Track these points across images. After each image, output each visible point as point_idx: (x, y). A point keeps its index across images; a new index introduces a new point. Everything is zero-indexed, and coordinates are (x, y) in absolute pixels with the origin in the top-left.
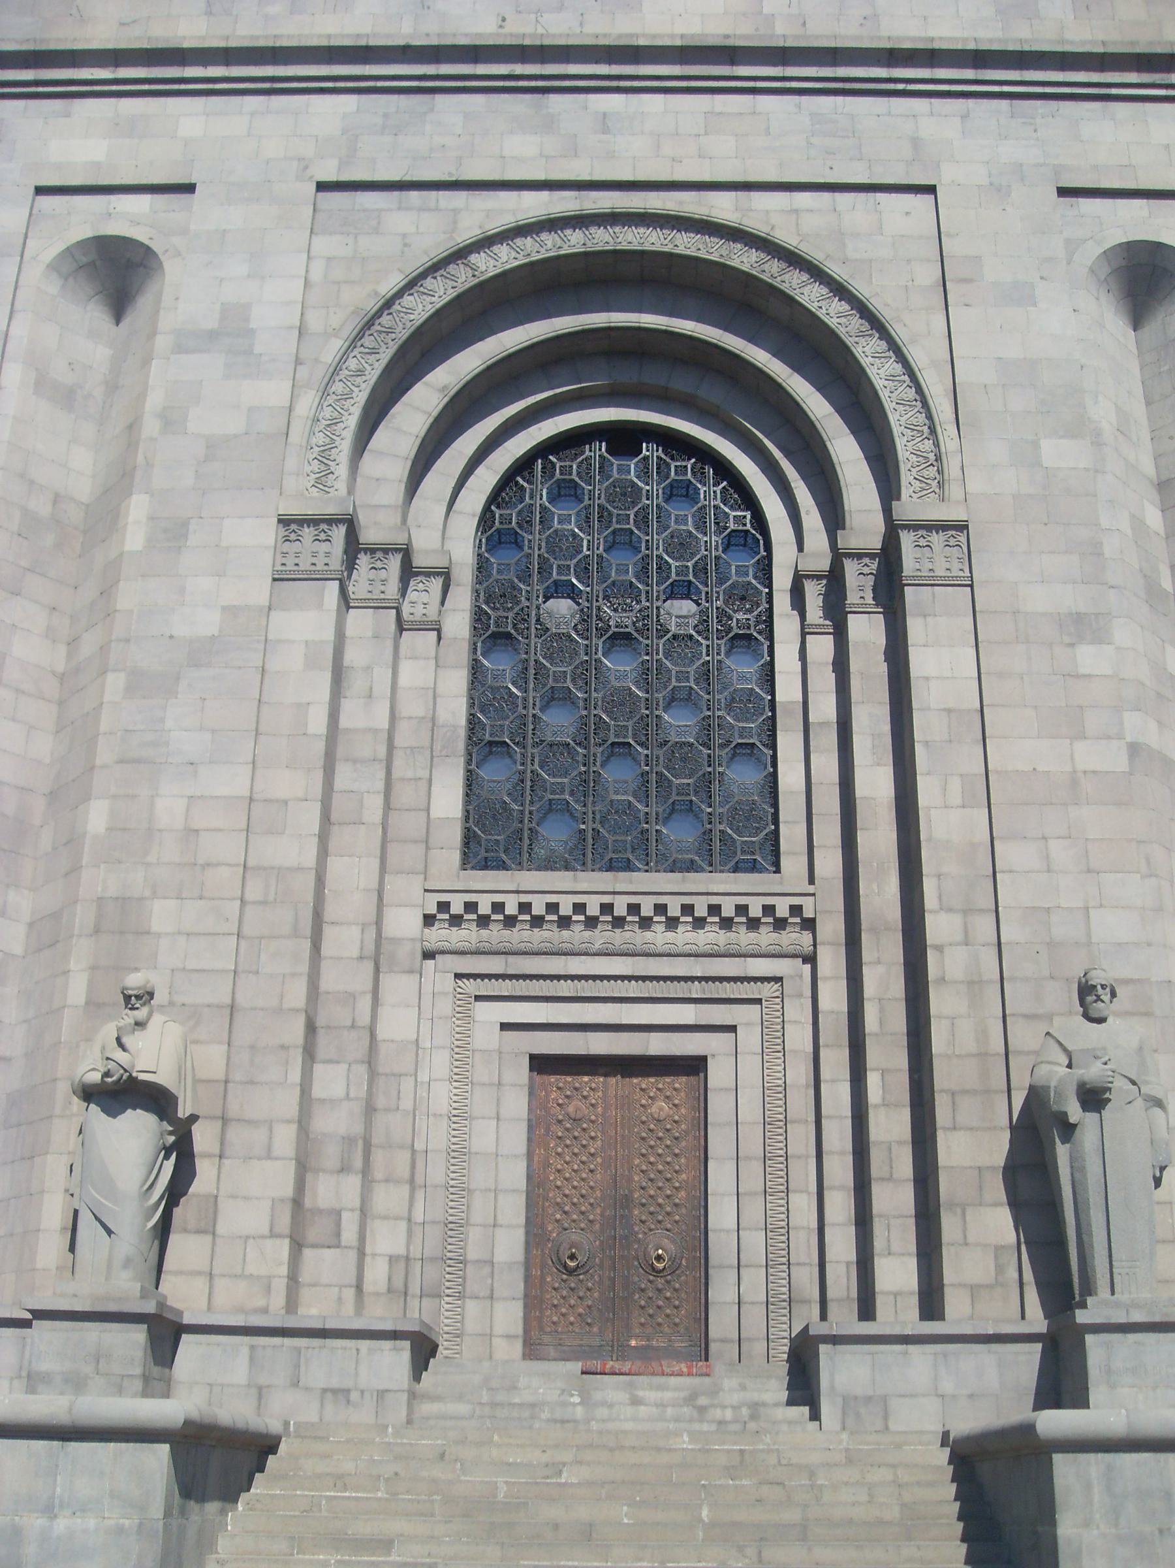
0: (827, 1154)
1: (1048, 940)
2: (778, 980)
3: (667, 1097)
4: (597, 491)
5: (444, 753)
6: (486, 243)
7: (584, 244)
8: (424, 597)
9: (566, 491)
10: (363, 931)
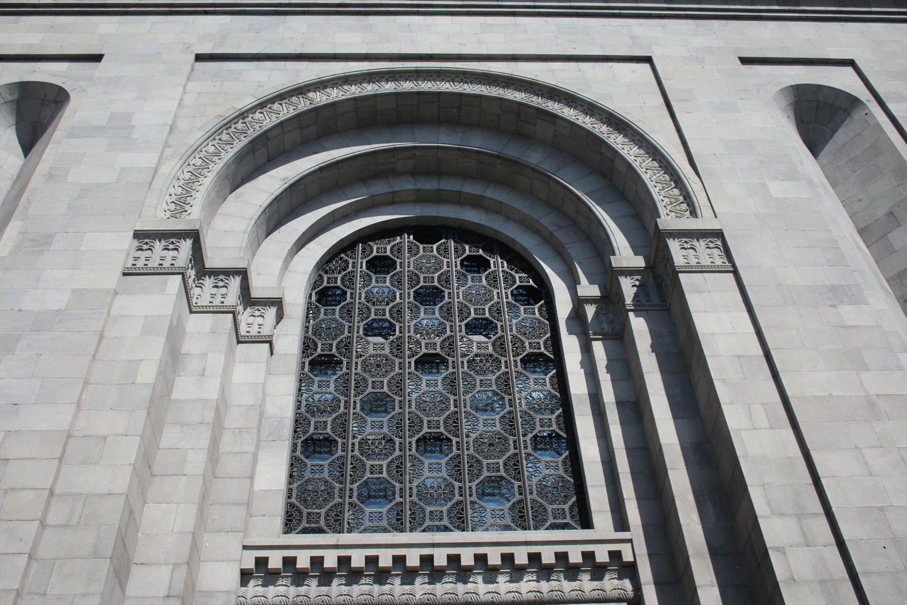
1: (892, 537)
4: (407, 263)
5: (270, 438)
6: (321, 85)
7: (395, 88)
8: (259, 320)
9: (380, 265)
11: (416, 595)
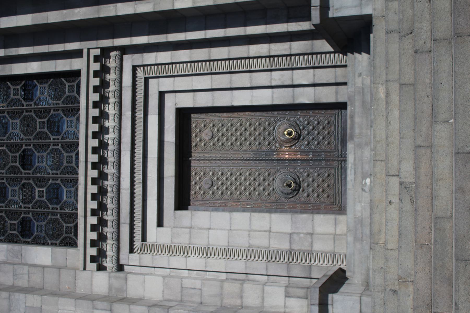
0: (226, 34)
2: (134, 68)
3: (200, 131)
5: (20, 257)
10: (97, 309)
11: (114, 172)
